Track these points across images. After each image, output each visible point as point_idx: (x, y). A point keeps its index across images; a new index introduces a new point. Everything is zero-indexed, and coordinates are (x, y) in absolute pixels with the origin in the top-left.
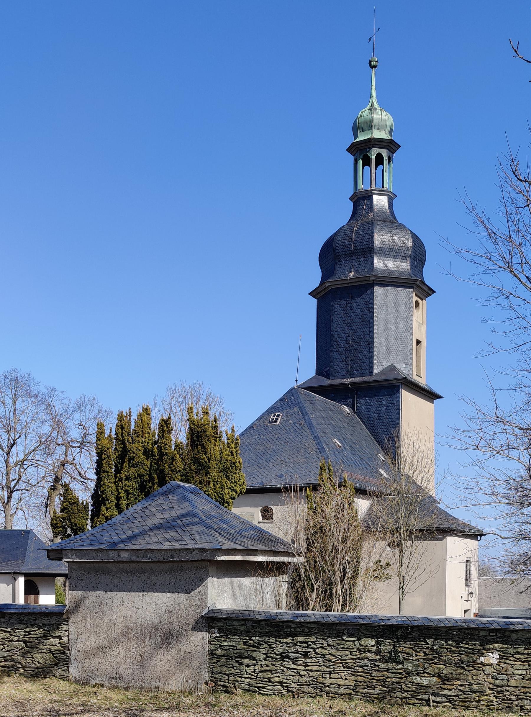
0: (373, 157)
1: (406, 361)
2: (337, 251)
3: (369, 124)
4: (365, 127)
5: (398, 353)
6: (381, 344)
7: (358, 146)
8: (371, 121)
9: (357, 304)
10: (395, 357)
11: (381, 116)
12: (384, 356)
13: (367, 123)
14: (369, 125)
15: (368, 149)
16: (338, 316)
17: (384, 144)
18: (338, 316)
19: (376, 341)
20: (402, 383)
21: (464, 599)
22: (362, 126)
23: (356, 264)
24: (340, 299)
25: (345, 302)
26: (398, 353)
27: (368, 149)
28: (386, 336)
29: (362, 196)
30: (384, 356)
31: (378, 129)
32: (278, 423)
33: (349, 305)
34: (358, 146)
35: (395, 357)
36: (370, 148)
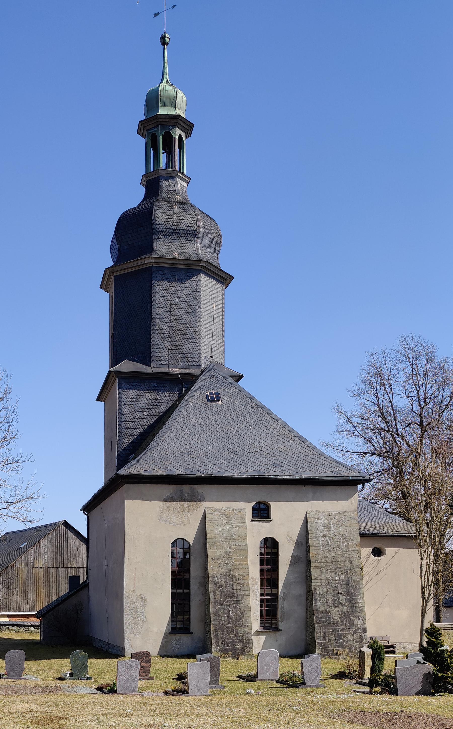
0: (177, 137)
2: (157, 226)
3: (172, 100)
4: (167, 102)
7: (161, 120)
8: (175, 99)
9: (182, 289)
11: (181, 97)
13: (170, 99)
14: (173, 103)
15: (171, 127)
16: (160, 298)
17: (186, 127)
18: (160, 298)
22: (165, 100)
23: (177, 245)
24: (163, 281)
25: (168, 285)
27: (171, 127)
29: (164, 175)
31: (180, 109)
32: (220, 402)
33: (173, 288)
34: (161, 120)
36: (174, 127)
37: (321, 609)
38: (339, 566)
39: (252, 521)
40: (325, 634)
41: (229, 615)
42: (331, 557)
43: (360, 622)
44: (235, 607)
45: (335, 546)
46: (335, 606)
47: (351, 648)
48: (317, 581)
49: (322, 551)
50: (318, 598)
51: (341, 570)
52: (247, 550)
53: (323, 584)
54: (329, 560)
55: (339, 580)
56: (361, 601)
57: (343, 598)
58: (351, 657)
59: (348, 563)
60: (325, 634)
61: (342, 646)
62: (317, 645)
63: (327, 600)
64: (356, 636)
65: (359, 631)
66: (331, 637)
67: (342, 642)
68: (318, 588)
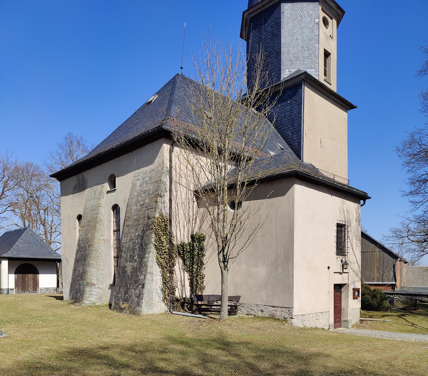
1: (312, 66)
5: (304, 59)
6: (288, 53)
10: (302, 63)
12: (291, 63)
19: (284, 50)
20: (304, 81)
21: (332, 270)
26: (304, 59)
28: (293, 45)
30: (291, 63)
35: (302, 63)
37: (122, 264)
38: (140, 223)
39: (108, 192)
40: (120, 288)
41: (79, 271)
42: (137, 215)
43: (142, 277)
44: (83, 264)
45: (141, 203)
46: (130, 261)
47: (131, 303)
48: (125, 238)
49: (133, 210)
50: (122, 254)
51: (141, 226)
52: (97, 217)
53: (128, 241)
54: (135, 217)
55: (138, 235)
56: (147, 255)
57: (136, 253)
58: (130, 313)
59: (146, 218)
60: (120, 288)
61: (126, 300)
62: (113, 298)
63: (127, 256)
64: (137, 291)
65: (140, 286)
66: (122, 290)
67: (127, 297)
68: (124, 245)
